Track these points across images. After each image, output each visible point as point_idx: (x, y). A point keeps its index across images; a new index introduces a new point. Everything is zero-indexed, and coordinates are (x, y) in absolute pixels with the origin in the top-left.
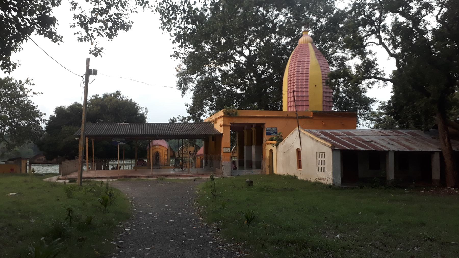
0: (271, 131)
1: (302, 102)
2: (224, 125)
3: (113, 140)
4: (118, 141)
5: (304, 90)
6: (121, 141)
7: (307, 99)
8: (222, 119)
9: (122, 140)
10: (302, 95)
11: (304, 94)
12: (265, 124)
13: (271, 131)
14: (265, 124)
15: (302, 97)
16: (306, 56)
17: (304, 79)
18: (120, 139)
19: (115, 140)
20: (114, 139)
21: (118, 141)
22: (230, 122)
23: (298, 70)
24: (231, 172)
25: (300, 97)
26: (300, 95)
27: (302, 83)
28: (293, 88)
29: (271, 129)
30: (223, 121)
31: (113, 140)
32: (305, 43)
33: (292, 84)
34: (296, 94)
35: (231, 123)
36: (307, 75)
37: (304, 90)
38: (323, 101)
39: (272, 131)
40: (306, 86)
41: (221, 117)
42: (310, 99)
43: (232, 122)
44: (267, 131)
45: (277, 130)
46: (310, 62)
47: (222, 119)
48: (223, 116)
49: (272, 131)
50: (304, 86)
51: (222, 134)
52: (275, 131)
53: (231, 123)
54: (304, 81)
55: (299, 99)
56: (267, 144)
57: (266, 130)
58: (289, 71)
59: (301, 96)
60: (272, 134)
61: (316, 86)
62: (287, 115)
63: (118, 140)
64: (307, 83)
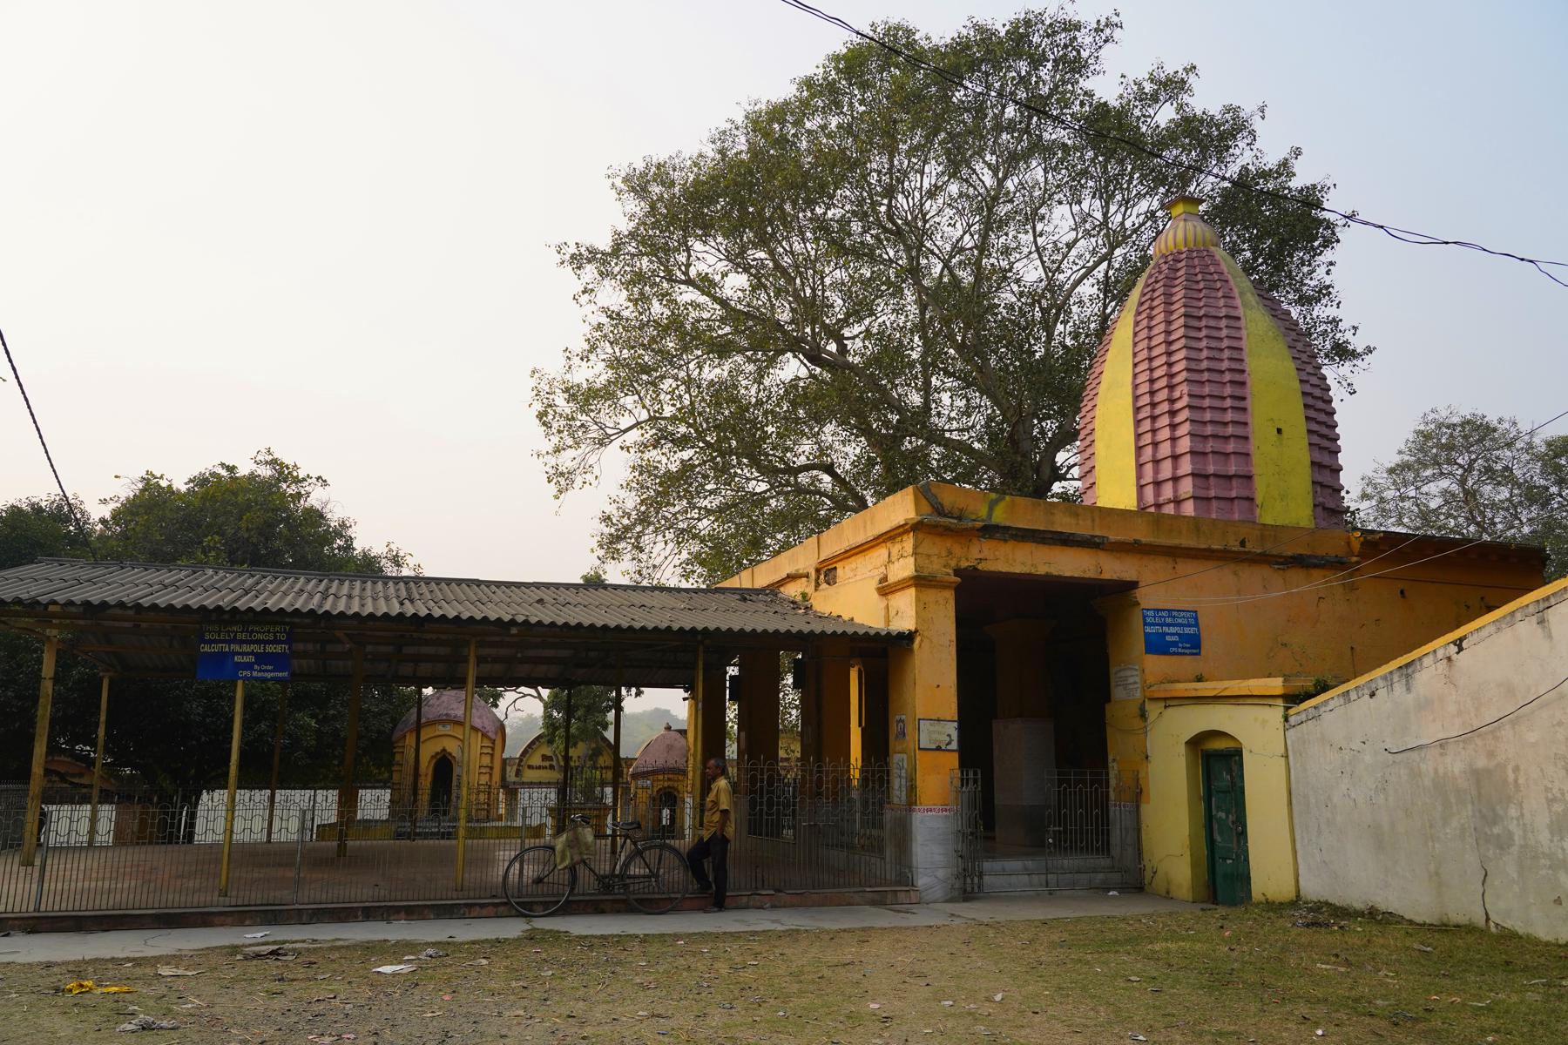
0: (1166, 629)
1: (1222, 504)
2: (924, 578)
3: (206, 649)
4: (243, 653)
5: (1231, 447)
6: (262, 659)
7: (1245, 493)
8: (908, 543)
9: (270, 649)
10: (1221, 470)
11: (1232, 469)
12: (1133, 585)
13: (1166, 629)
14: (1133, 585)
15: (1222, 481)
16: (1220, 294)
17: (1224, 398)
18: (258, 642)
19: (215, 648)
20: (210, 642)
21: (243, 653)
22: (953, 563)
23: (1193, 354)
24: (964, 874)
25: (1212, 481)
26: (1211, 469)
27: (1218, 416)
28: (1173, 439)
29: (1169, 620)
30: (915, 553)
31: (206, 649)
32: (1191, 245)
33: (1165, 420)
34: (1193, 463)
35: (957, 572)
36: (1237, 377)
37: (1231, 447)
38: (1315, 506)
39: (1172, 630)
40: (1239, 431)
41: (906, 532)
42: (1260, 490)
43: (964, 564)
44: (1148, 630)
45: (1197, 625)
46: (1242, 323)
47: (908, 543)
48: (916, 528)
49: (1172, 630)
50: (1230, 430)
51: (907, 638)
52: (1187, 630)
53: (957, 572)
54: (1228, 403)
55: (1208, 489)
56: (1153, 710)
57: (1145, 624)
58: (1135, 365)
59: (1215, 475)
60: (1175, 644)
61: (1279, 431)
62: (1243, 543)
63: (236, 647)
64: (1238, 417)
